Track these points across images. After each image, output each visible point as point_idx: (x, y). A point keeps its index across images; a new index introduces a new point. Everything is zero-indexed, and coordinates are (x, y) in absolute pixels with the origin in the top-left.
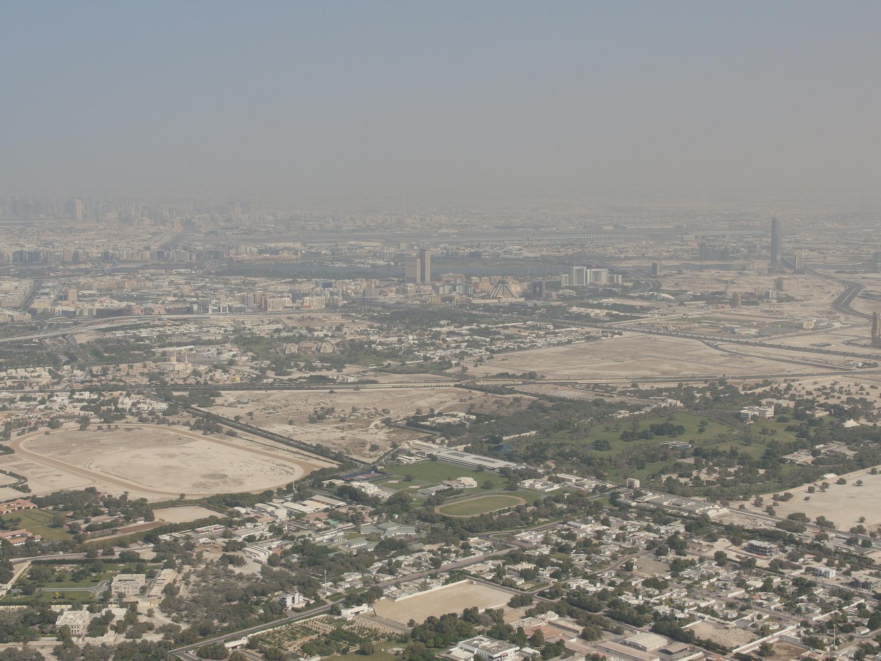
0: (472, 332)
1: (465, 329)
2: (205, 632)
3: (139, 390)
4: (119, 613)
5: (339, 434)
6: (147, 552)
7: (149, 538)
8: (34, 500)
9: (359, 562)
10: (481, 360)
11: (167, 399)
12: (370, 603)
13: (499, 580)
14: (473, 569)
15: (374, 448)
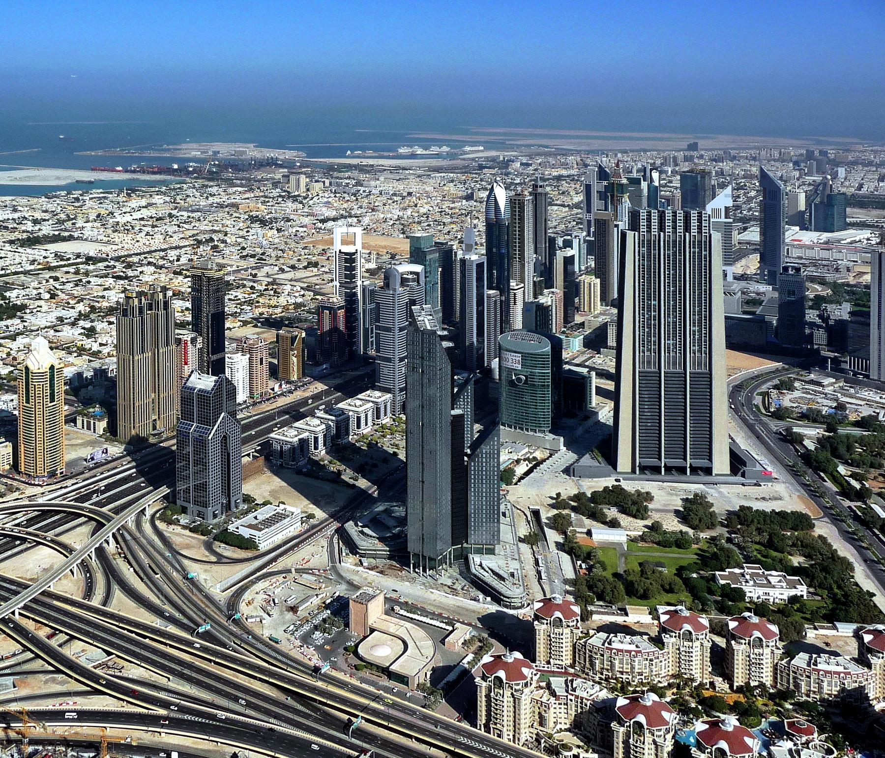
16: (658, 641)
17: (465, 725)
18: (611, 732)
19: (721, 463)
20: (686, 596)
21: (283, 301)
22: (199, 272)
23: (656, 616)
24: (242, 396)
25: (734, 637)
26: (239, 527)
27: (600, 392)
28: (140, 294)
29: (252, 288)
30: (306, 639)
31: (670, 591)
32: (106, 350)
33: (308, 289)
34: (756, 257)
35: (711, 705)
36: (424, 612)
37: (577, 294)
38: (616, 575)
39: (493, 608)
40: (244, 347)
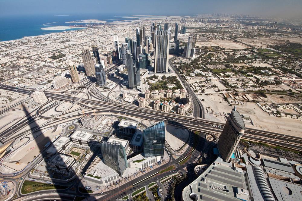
0: (280, 34)
1: (279, 34)
2: (228, 62)
3: (227, 36)
4: (218, 59)
5: (253, 44)
6: (223, 54)
7: (224, 52)
8: (212, 46)
9: (250, 59)
10: (280, 38)
11: (231, 38)
12: (251, 63)
13: (272, 64)
14: (268, 63)
15: (258, 46)
16: (159, 94)
17: (137, 107)
18: (153, 105)
19: (167, 71)
20: (162, 88)
21: (107, 51)
22: (93, 46)
23: (158, 91)
24: (104, 67)
25: (167, 92)
26: (107, 86)
27: (153, 62)
28: (84, 51)
29: (102, 49)
30: (118, 100)
31: (160, 88)
32: (81, 61)
33: (111, 48)
34: (174, 39)
35: (164, 100)
36: (132, 94)
37: (150, 47)
38: (154, 87)
39: (139, 93)
40: (103, 59)
